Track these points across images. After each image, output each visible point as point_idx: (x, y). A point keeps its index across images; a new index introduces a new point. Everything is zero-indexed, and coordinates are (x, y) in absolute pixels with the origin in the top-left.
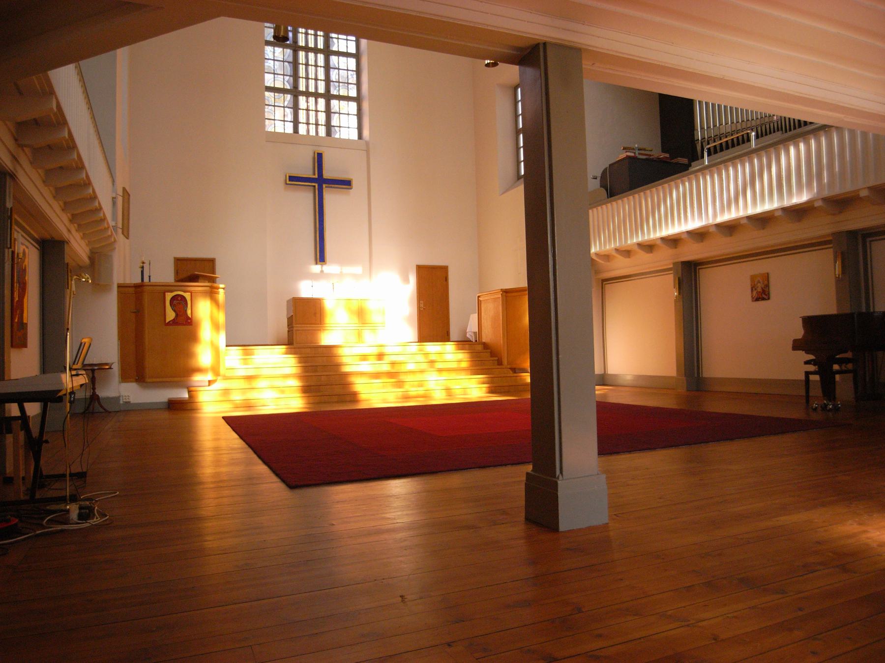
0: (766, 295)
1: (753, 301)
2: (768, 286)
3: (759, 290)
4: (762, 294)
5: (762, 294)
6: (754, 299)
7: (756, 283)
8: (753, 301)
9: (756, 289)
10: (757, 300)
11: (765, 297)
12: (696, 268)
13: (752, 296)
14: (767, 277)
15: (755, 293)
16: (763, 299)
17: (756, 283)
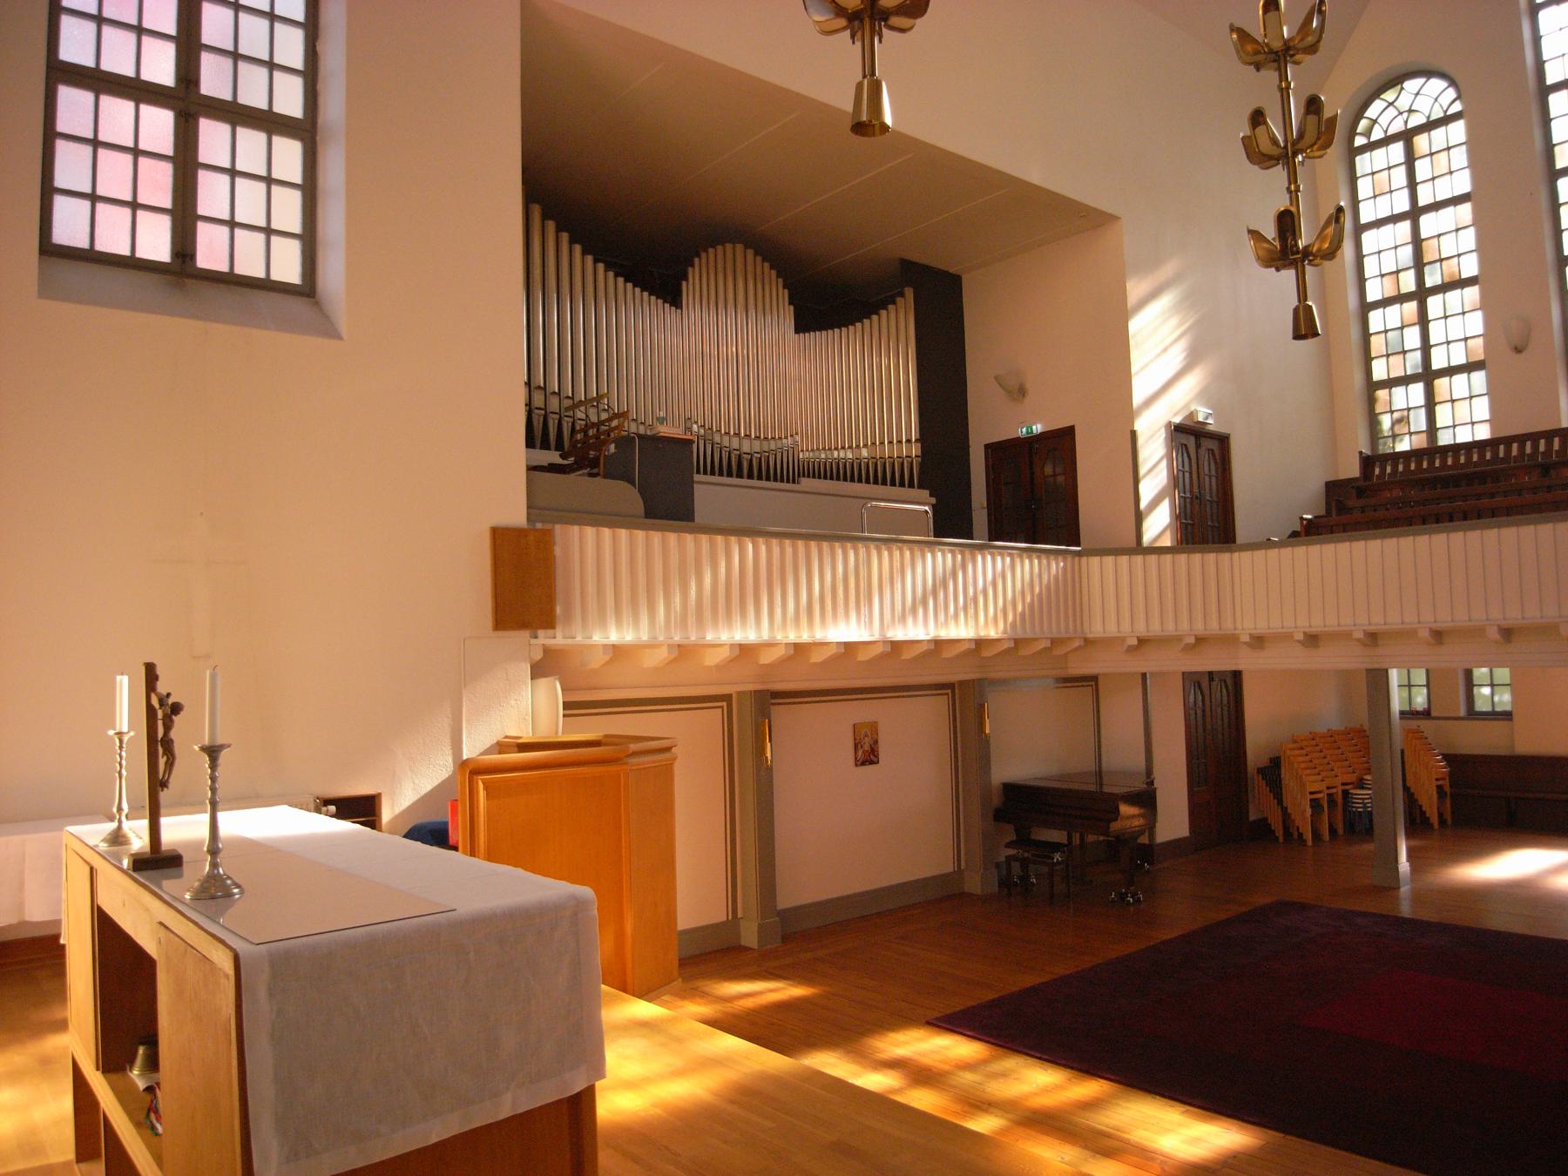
0: (876, 757)
1: (856, 765)
2: (876, 742)
3: (867, 747)
4: (868, 756)
5: (868, 756)
6: (859, 763)
7: (862, 737)
8: (856, 765)
9: (862, 747)
10: (863, 764)
11: (876, 760)
12: (723, 701)
13: (856, 758)
14: (874, 727)
15: (860, 752)
16: (872, 763)
17: (862, 737)
